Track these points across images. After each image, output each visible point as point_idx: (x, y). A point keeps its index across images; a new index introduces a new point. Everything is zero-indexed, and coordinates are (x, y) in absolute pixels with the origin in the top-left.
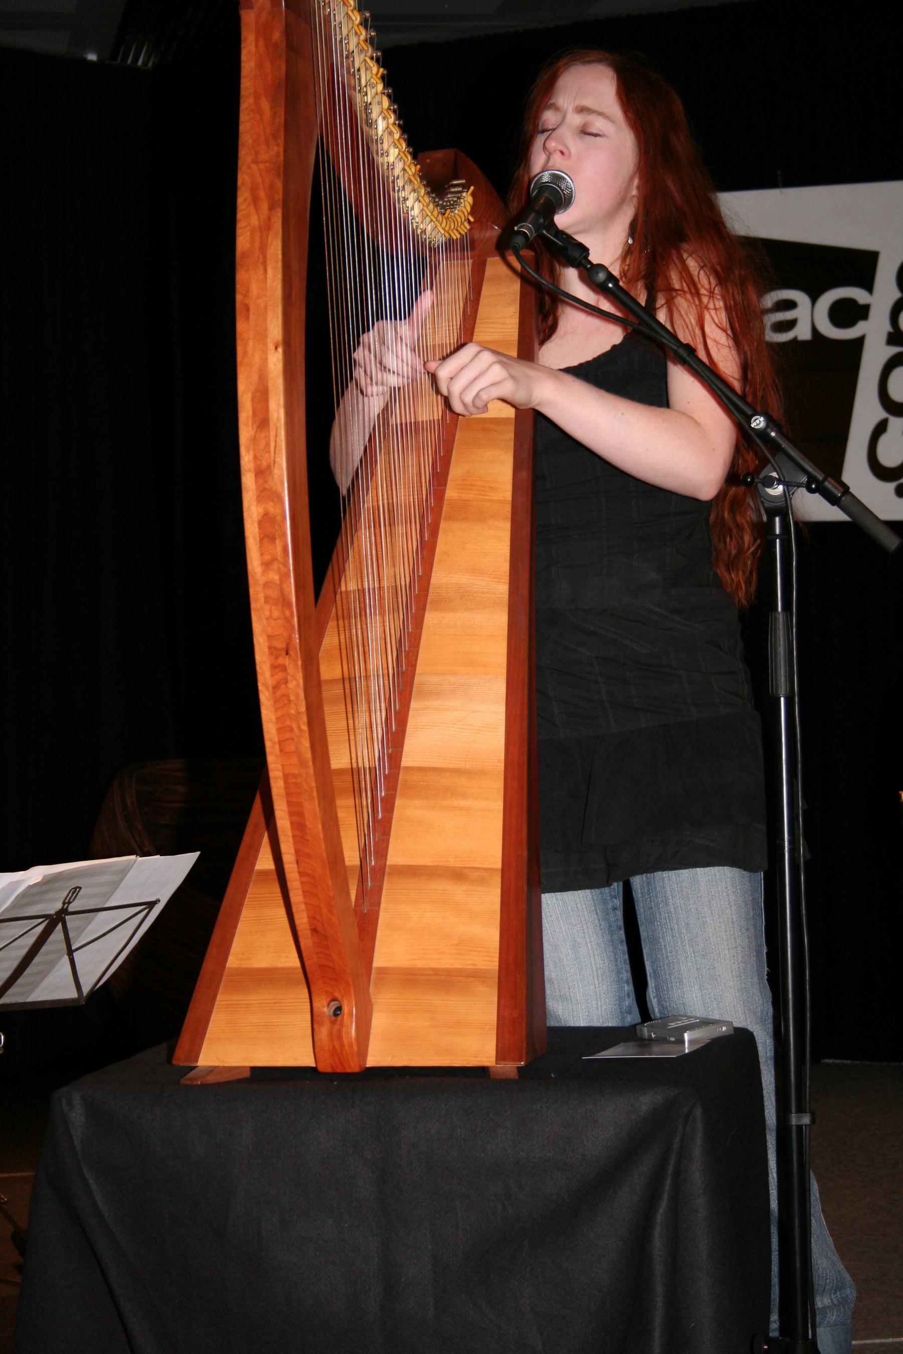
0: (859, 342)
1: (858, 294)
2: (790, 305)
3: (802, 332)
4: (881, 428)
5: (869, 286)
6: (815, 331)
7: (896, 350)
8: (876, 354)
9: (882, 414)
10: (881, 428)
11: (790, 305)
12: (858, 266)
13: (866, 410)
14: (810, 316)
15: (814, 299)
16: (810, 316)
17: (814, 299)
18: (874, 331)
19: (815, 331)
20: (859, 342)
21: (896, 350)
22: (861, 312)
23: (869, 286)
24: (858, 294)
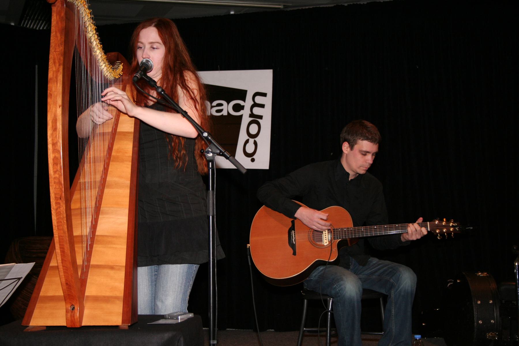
0: (241, 116)
2: (221, 105)
3: (225, 113)
4: (247, 142)
5: (244, 101)
6: (228, 112)
8: (246, 120)
9: (248, 138)
10: (247, 142)
11: (221, 105)
12: (241, 94)
13: (243, 136)
14: (227, 108)
15: (228, 104)
16: (227, 108)
17: (228, 104)
18: (245, 113)
19: (228, 112)
20: (241, 116)
22: (242, 108)
23: (244, 100)
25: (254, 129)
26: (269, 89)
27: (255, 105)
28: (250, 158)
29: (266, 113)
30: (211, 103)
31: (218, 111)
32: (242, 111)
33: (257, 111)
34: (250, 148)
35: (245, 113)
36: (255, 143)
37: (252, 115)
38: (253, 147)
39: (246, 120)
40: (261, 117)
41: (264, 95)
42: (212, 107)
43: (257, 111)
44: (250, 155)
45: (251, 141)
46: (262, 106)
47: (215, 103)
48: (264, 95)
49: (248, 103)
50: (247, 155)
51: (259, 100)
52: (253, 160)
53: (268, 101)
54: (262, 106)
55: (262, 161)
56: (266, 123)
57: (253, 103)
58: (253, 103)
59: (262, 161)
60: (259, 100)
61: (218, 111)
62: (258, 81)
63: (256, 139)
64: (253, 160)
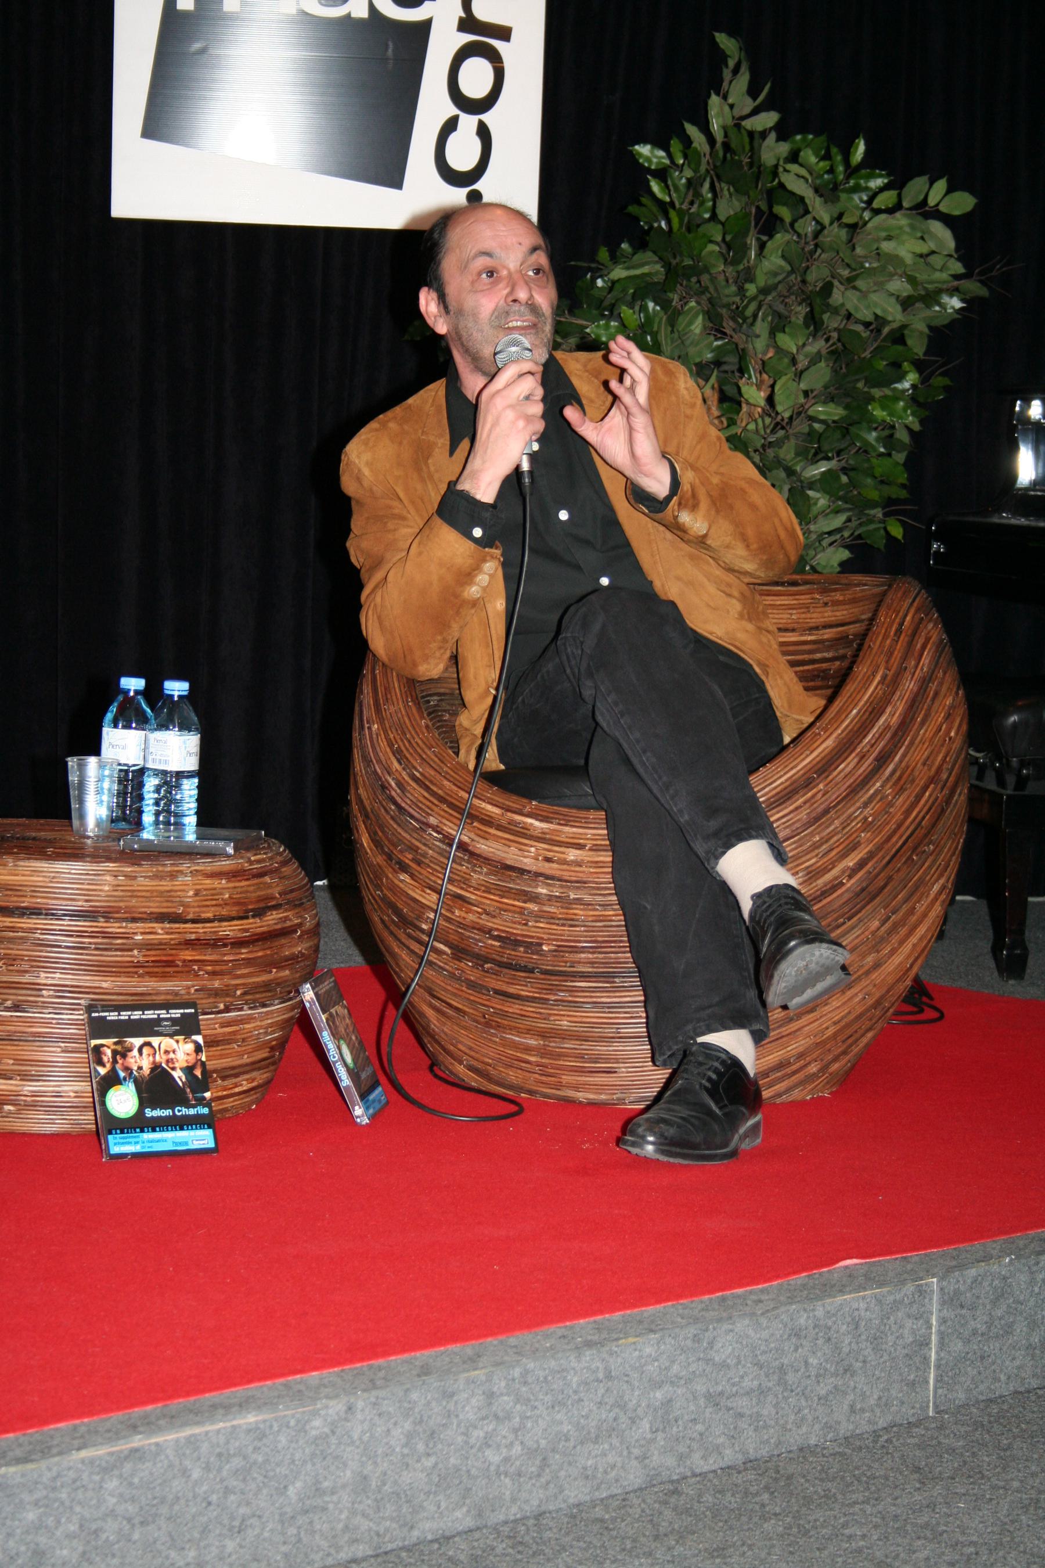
0: (425, 27)
4: (450, 126)
7: (468, 38)
8: (445, 41)
9: (451, 110)
10: (450, 126)
13: (433, 105)
19: (372, 8)
21: (468, 38)
25: (476, 77)
34: (463, 152)
36: (484, 133)
38: (477, 145)
39: (445, 41)
40: (504, 33)
45: (468, 123)
50: (451, 176)
56: (526, 57)
63: (486, 117)
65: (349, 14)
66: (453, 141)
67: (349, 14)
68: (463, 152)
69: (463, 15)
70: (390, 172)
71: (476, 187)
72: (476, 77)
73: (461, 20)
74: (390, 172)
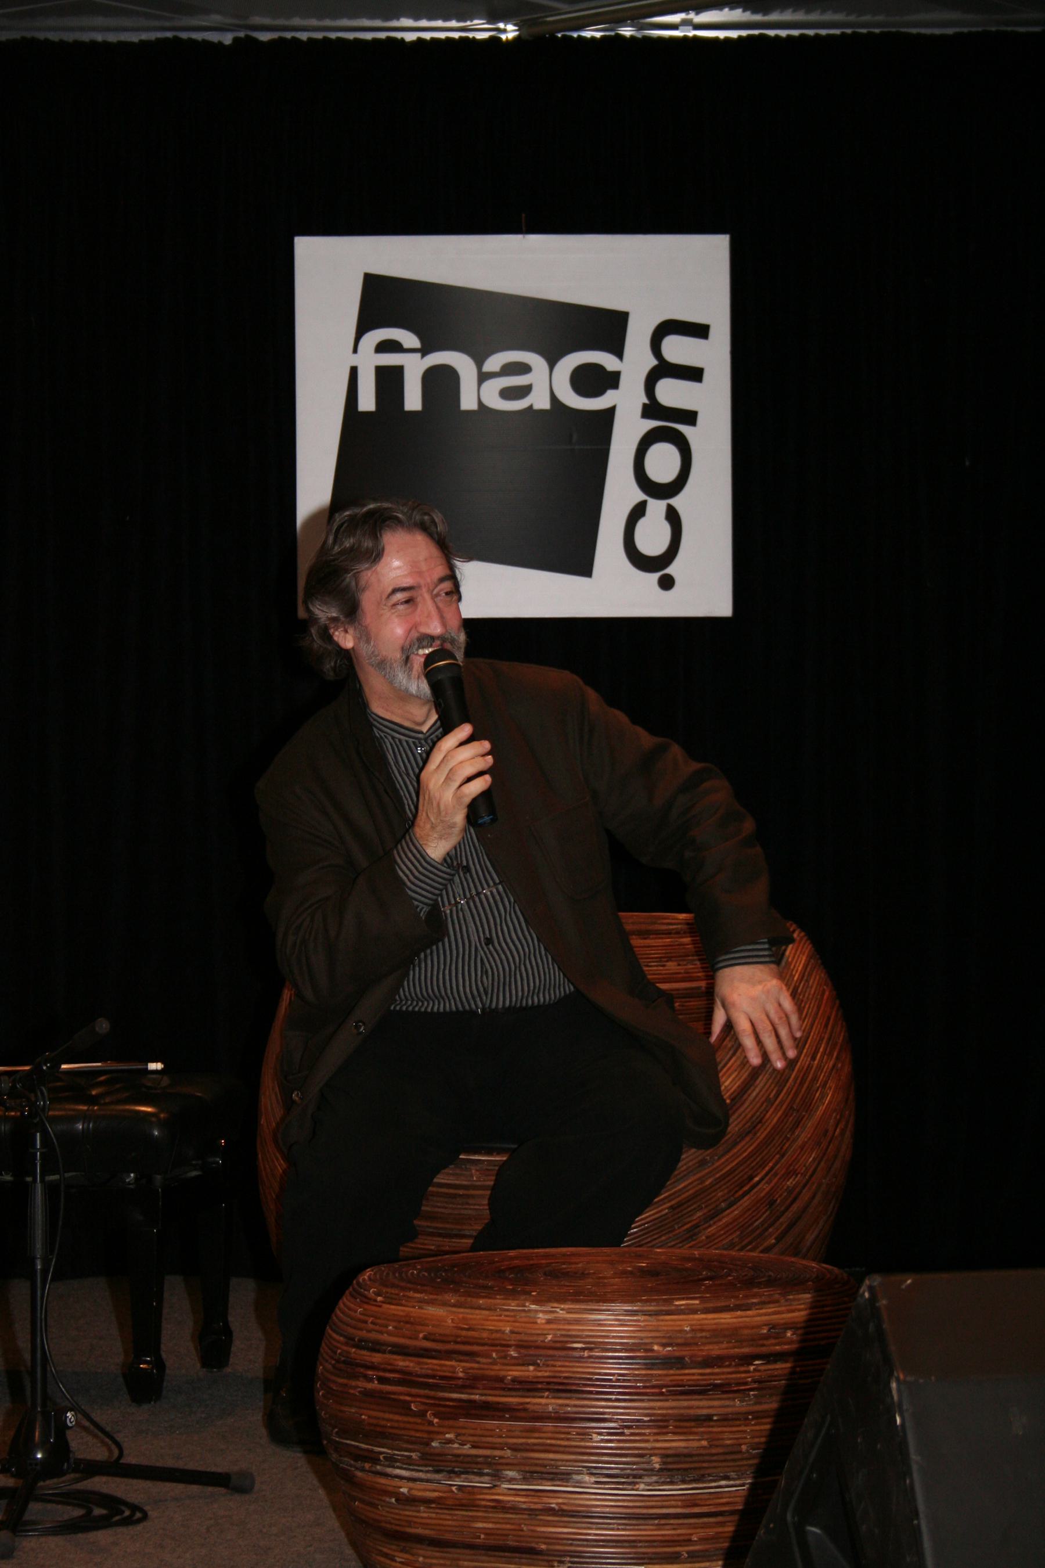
0: (611, 412)
1: (607, 360)
2: (524, 369)
3: (540, 400)
4: (638, 512)
5: (619, 353)
6: (553, 398)
9: (641, 496)
10: (638, 512)
11: (524, 369)
12: (607, 328)
13: (620, 491)
14: (549, 383)
15: (552, 364)
16: (549, 383)
17: (552, 364)
18: (626, 402)
19: (553, 398)
20: (611, 412)
22: (612, 380)
23: (619, 353)
24: (607, 360)
25: (662, 463)
26: (714, 306)
27: (663, 370)
28: (655, 577)
29: (712, 402)
30: (479, 364)
31: (507, 394)
32: (610, 393)
33: (672, 393)
34: (653, 537)
35: (626, 402)
36: (673, 517)
37: (652, 409)
40: (690, 417)
41: (700, 331)
42: (483, 377)
43: (672, 393)
44: (657, 565)
45: (656, 508)
46: (694, 374)
47: (494, 362)
48: (700, 331)
49: (635, 361)
51: (678, 349)
52: (667, 583)
53: (714, 355)
54: (694, 374)
55: (704, 587)
56: (713, 441)
57: (654, 362)
58: (654, 362)
59: (704, 587)
60: (678, 349)
61: (507, 394)
62: (672, 279)
63: (676, 502)
64: (667, 583)
65: (531, 406)
66: (641, 526)
67: (531, 406)
68: (653, 537)
69: (647, 401)
70: (579, 561)
71: (668, 571)
72: (662, 463)
73: (645, 405)
74: (579, 561)
